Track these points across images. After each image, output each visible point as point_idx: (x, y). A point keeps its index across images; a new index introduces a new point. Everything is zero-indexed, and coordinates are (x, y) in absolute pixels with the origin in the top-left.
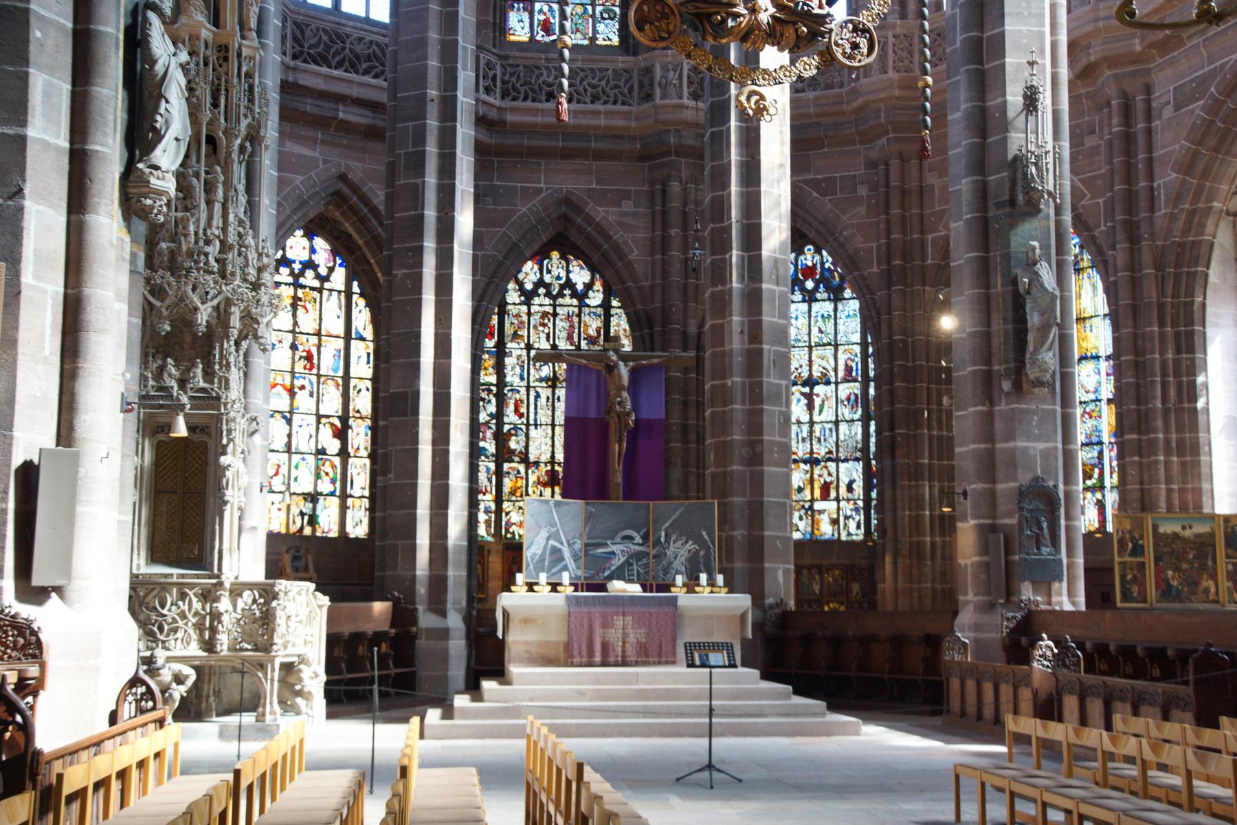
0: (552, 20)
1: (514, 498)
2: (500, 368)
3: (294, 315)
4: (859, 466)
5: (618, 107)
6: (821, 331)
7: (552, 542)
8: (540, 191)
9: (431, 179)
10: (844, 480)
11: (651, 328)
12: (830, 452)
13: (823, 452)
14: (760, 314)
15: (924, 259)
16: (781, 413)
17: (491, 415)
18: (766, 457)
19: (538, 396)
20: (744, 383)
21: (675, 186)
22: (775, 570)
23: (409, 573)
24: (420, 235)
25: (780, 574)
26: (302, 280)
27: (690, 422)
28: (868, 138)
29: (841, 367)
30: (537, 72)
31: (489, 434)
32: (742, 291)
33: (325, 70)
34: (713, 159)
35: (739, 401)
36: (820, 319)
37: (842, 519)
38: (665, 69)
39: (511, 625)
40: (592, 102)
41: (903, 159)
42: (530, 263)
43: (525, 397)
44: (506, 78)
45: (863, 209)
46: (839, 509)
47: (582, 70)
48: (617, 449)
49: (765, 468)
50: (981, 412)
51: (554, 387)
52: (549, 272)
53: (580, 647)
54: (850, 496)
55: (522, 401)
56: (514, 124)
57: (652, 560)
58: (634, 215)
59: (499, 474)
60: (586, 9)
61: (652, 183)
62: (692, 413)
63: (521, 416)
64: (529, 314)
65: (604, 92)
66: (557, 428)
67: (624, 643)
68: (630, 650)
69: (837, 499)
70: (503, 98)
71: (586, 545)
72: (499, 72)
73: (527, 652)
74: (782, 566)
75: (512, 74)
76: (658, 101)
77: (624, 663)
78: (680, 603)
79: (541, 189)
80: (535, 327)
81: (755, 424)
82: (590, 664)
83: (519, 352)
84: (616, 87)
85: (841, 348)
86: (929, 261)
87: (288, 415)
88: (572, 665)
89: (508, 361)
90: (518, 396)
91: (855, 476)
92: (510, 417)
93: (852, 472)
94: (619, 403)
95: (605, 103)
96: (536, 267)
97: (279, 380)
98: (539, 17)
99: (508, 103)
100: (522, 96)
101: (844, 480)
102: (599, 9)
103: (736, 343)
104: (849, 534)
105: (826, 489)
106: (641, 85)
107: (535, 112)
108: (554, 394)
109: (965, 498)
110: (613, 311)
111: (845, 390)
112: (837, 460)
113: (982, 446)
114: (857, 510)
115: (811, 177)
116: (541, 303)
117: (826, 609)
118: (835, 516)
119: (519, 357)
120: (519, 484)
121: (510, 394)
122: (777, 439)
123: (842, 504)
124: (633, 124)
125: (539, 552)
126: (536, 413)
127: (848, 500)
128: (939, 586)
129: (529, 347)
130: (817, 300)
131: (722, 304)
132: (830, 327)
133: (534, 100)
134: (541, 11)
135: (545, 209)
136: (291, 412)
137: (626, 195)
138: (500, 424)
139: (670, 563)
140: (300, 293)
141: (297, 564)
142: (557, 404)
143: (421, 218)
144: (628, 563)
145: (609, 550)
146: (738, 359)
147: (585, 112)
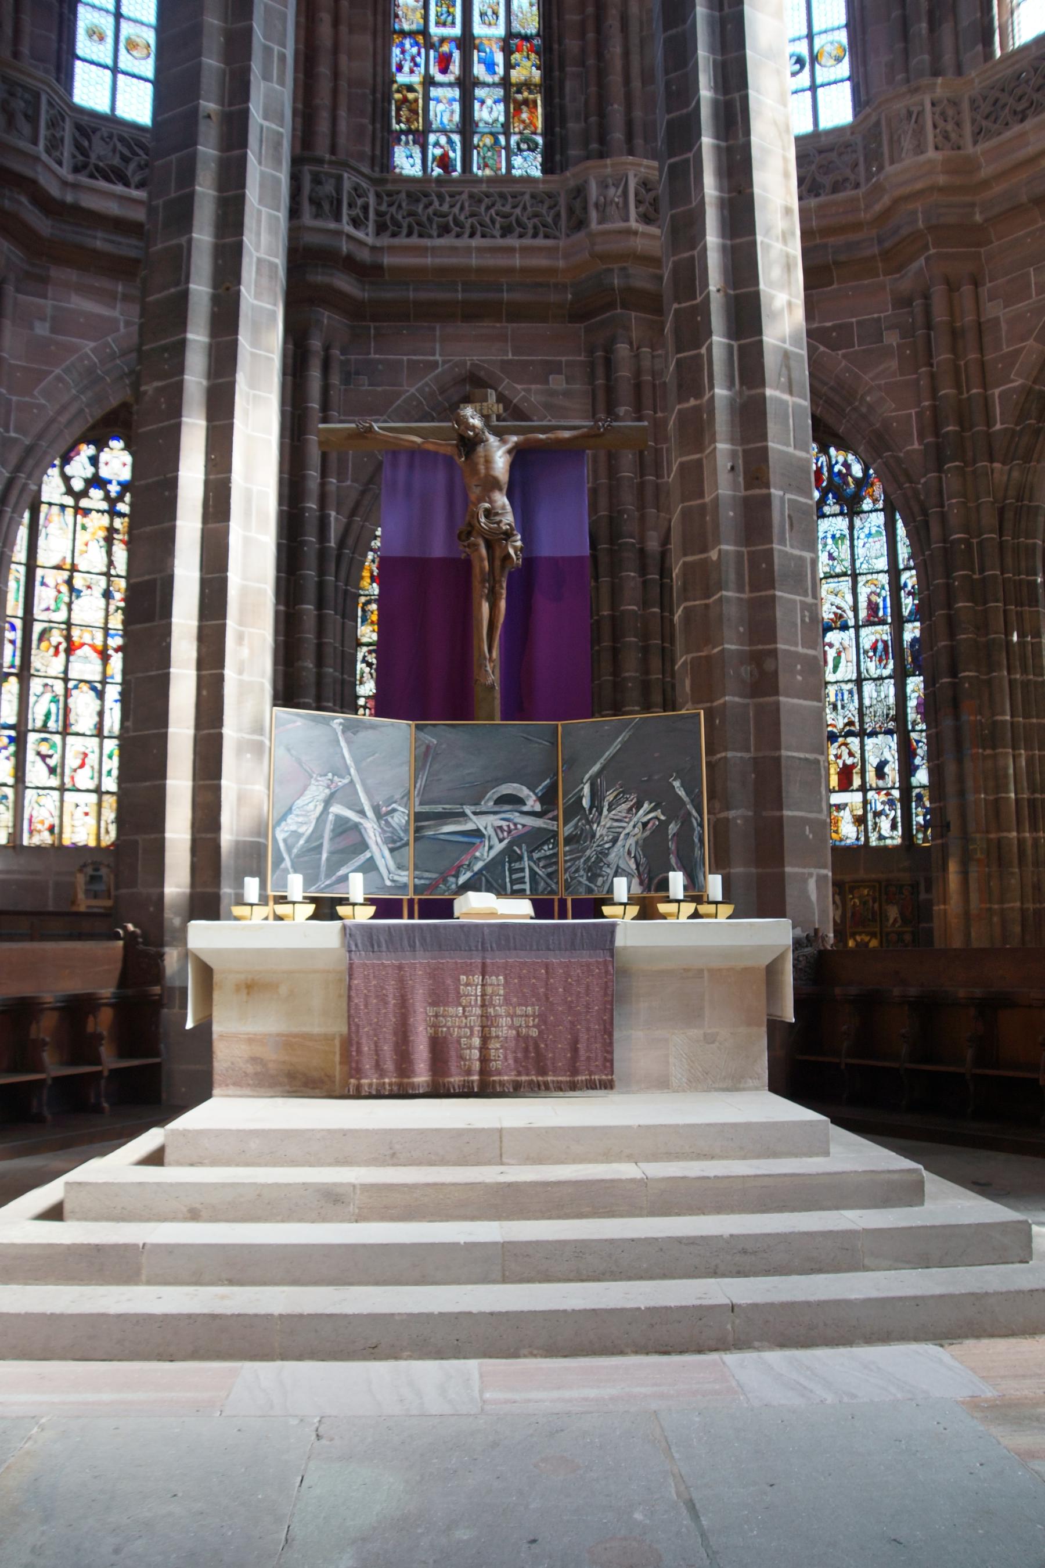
0: (451, 154)
3: (109, 553)
4: (893, 742)
5: (540, 242)
6: (831, 557)
7: (336, 809)
8: (435, 365)
9: (203, 236)
10: (873, 761)
12: (851, 723)
13: (840, 723)
14: (764, 437)
15: (989, 422)
16: (805, 606)
18: (783, 680)
20: (739, 555)
21: (623, 349)
22: (804, 880)
23: (154, 891)
24: (181, 322)
25: (812, 884)
28: (894, 259)
29: (863, 604)
30: (424, 200)
32: (732, 402)
33: (119, 189)
34: (673, 205)
35: (732, 585)
36: (830, 541)
37: (870, 816)
38: (604, 185)
39: (216, 996)
40: (503, 236)
41: (952, 287)
44: (383, 208)
45: (894, 364)
46: (865, 802)
47: (488, 195)
48: (488, 613)
49: (782, 699)
53: (377, 1051)
54: (881, 783)
56: (396, 270)
57: (562, 849)
58: (566, 394)
60: (496, 141)
61: (591, 352)
62: (656, 662)
67: (485, 1039)
68: (501, 1059)
69: (863, 789)
70: (378, 234)
71: (419, 817)
72: (372, 200)
73: (254, 1060)
74: (815, 871)
75: (390, 205)
76: (594, 226)
77: (486, 1090)
78: (620, 941)
79: (436, 363)
81: (761, 623)
82: (403, 1093)
84: (536, 215)
85: (861, 579)
86: (998, 426)
87: (99, 686)
88: (358, 1095)
91: (887, 755)
93: (883, 749)
94: (488, 513)
95: (521, 236)
97: (87, 638)
99: (385, 241)
101: (873, 761)
102: (514, 139)
103: (724, 486)
104: (881, 837)
105: (846, 773)
106: (571, 211)
107: (423, 251)
111: (869, 636)
112: (862, 734)
114: (891, 803)
117: (851, 943)
118: (860, 812)
122: (800, 649)
123: (870, 795)
124: (561, 264)
125: (307, 830)
127: (878, 790)
128: (1030, 906)
130: (823, 516)
131: (697, 429)
132: (843, 551)
133: (421, 236)
135: (443, 391)
136: (104, 682)
137: (555, 368)
139: (604, 853)
141: (96, 887)
143: (184, 296)
144: (510, 855)
145: (469, 826)
146: (729, 514)
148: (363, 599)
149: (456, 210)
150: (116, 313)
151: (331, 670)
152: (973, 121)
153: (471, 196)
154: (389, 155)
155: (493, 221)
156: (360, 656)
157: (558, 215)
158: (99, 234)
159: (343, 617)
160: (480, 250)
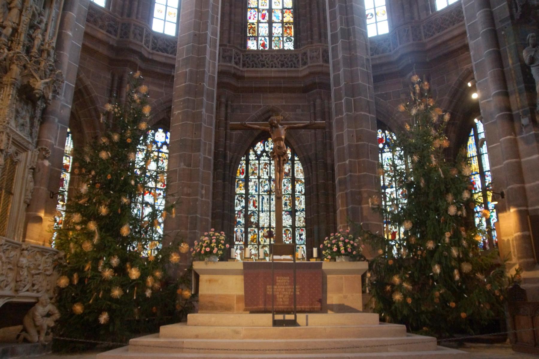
0: (266, 43)
1: (253, 243)
2: (246, 187)
5: (293, 69)
8: (260, 106)
11: (311, 163)
17: (243, 207)
19: (263, 198)
26: (161, 150)
27: (330, 203)
31: (242, 215)
33: (165, 54)
36: (386, 160)
40: (282, 67)
42: (259, 143)
43: (257, 199)
44: (245, 59)
50: (508, 139)
51: (270, 195)
52: (268, 146)
55: (256, 201)
56: (249, 78)
59: (246, 233)
63: (256, 207)
64: (259, 164)
65: (287, 64)
66: (272, 212)
72: (241, 56)
75: (247, 58)
80: (262, 169)
83: (255, 180)
89: (251, 184)
90: (254, 199)
92: (251, 208)
96: (262, 144)
98: (260, 42)
99: (245, 69)
100: (251, 66)
102: (285, 38)
106: (303, 59)
108: (270, 197)
109: (503, 197)
110: (295, 162)
113: (514, 160)
115: (379, 93)
116: (264, 159)
119: (255, 182)
120: (255, 237)
121: (251, 198)
126: (262, 206)
129: (259, 178)
130: (384, 152)
133: (256, 67)
134: (261, 40)
138: (247, 211)
140: (160, 155)
142: (271, 202)
147: (279, 71)
148: (237, 180)
149: (267, 60)
150: (162, 91)
151: (227, 201)
152: (424, 32)
153: (272, 56)
154: (246, 43)
155: (278, 63)
156: (236, 198)
157: (298, 61)
158: (159, 68)
159: (231, 185)
160: (275, 71)
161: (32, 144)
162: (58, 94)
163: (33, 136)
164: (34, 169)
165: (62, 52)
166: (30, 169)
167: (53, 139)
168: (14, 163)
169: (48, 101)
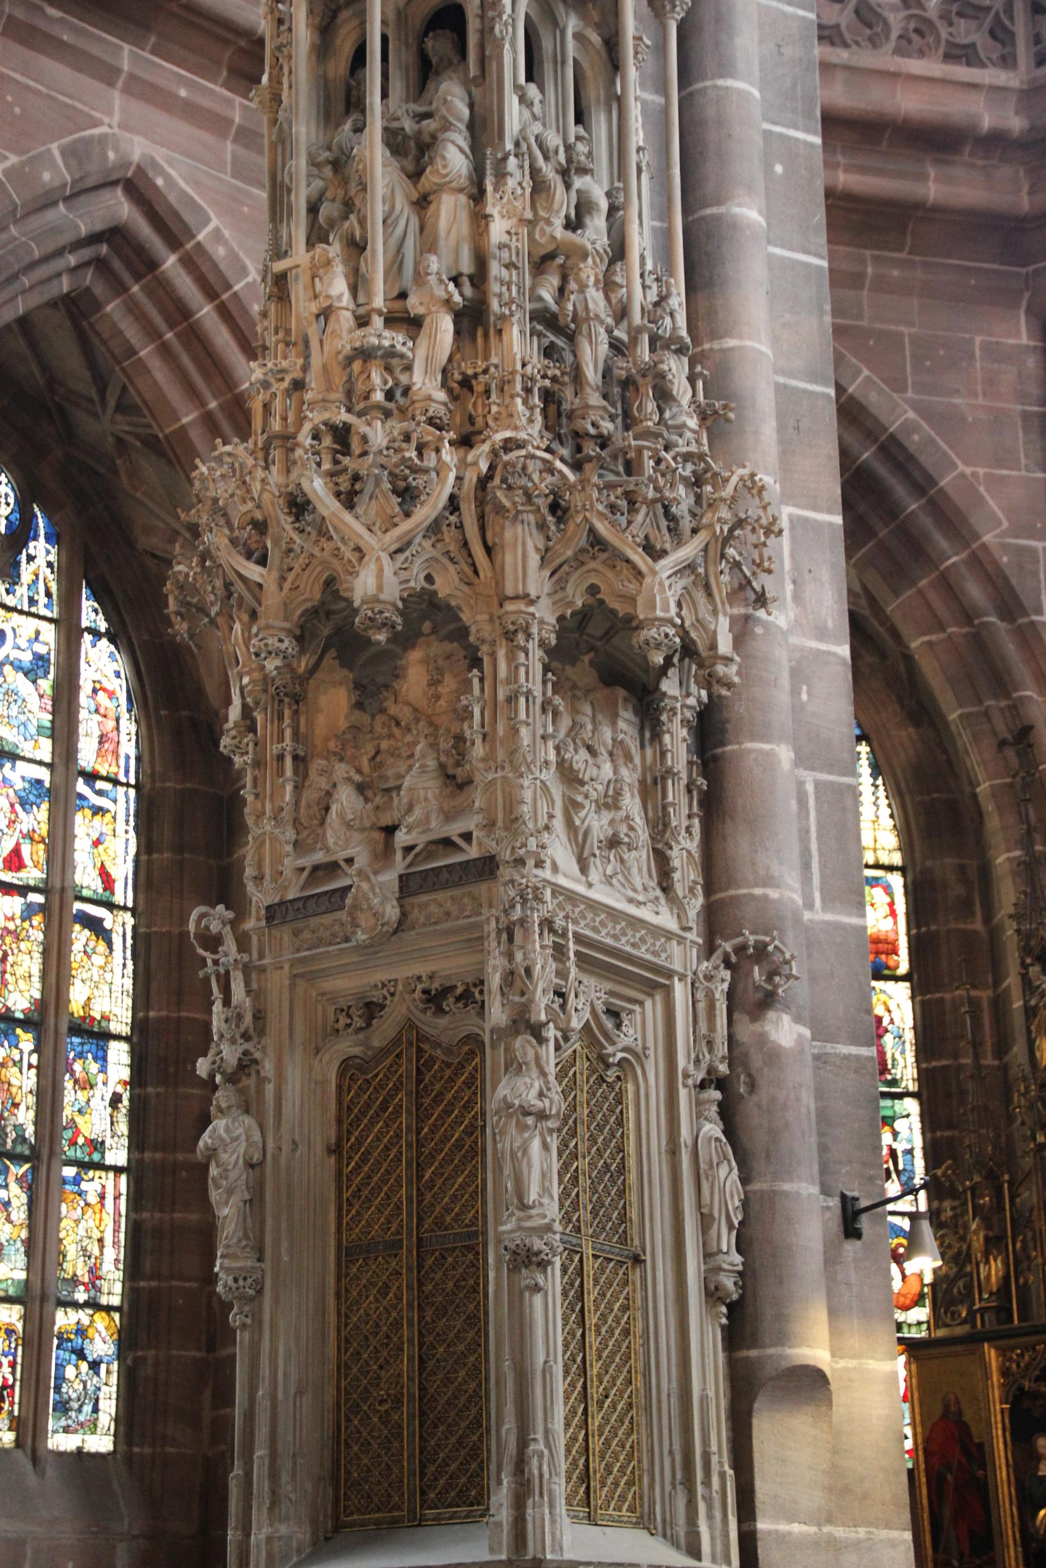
161: (681, 940)
162: (761, 600)
163: (680, 890)
164: (721, 1084)
165: (730, 343)
166: (702, 1086)
167: (792, 878)
168: (611, 1075)
169: (720, 669)
